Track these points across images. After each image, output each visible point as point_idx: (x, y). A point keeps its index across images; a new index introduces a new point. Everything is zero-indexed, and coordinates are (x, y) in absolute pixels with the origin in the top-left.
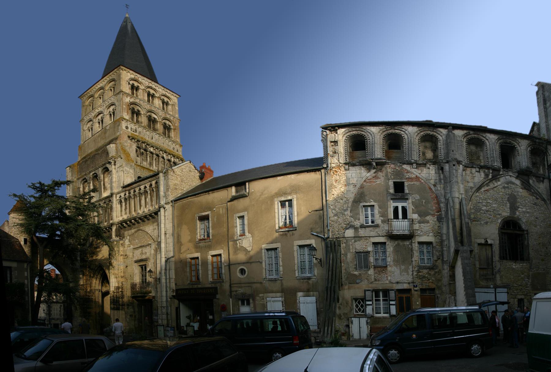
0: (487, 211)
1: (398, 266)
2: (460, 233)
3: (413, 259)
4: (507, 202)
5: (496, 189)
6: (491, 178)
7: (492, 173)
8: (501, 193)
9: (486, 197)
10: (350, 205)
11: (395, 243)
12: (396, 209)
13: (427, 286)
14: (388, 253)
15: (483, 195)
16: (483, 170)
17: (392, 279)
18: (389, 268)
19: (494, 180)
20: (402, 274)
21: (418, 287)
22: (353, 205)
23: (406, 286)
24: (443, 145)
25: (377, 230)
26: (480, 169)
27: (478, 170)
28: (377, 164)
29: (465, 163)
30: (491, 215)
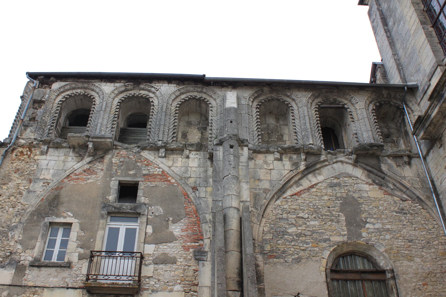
0: (299, 235)
2: (238, 281)
4: (340, 214)
5: (314, 190)
6: (304, 170)
7: (305, 160)
8: (326, 198)
9: (295, 207)
15: (289, 204)
16: (289, 155)
19: (309, 173)
22: (30, 221)
24: (217, 115)
25: (65, 273)
26: (281, 154)
27: (277, 155)
28: (96, 148)
29: (254, 145)
30: (307, 243)
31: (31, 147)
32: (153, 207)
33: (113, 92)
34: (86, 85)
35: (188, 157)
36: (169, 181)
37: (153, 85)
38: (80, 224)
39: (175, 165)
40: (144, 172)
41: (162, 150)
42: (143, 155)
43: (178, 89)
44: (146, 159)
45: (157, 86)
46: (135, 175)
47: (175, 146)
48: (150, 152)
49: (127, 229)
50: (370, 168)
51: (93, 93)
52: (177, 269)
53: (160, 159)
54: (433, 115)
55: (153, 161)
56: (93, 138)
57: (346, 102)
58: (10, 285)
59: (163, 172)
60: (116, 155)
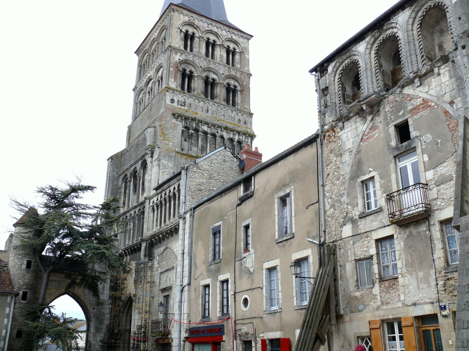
3: (435, 256)
11: (406, 233)
14: (397, 253)
17: (406, 298)
18: (401, 280)
20: (420, 288)
21: (448, 310)
23: (427, 310)
31: (333, 129)
32: (423, 137)
33: (366, 48)
34: (348, 54)
37: (392, 21)
38: (379, 174)
39: (431, 88)
40: (410, 108)
41: (417, 80)
42: (405, 93)
43: (412, 11)
44: (408, 95)
45: (395, 20)
46: (404, 115)
47: (425, 71)
48: (409, 86)
49: (412, 164)
53: (418, 89)
55: (414, 94)
56: (363, 101)
60: (386, 103)
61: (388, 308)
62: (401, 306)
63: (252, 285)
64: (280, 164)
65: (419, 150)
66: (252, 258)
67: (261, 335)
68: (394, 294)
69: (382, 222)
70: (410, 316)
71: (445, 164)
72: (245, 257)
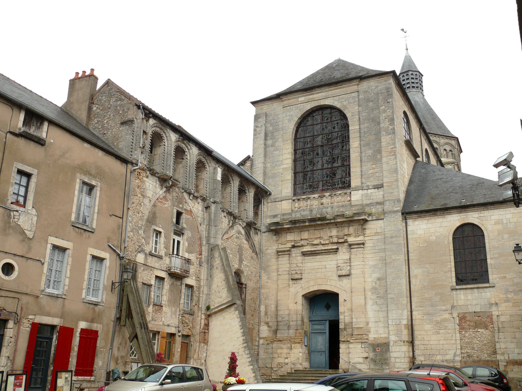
1: (171, 307)
10: (144, 223)
12: (174, 240)
13: (187, 333)
17: (165, 321)
18: (164, 308)
23: (173, 330)
34: (163, 128)
35: (198, 203)
36: (192, 216)
37: (190, 144)
41: (192, 196)
50: (247, 231)
51: (164, 135)
52: (194, 268)
54: (285, 226)
56: (173, 179)
57: (247, 189)
58: (144, 264)
59: (190, 209)
61: (155, 323)
62: (162, 324)
63: (27, 253)
64: (86, 145)
65: (185, 237)
66: (32, 220)
67: (30, 317)
68: (159, 316)
69: (161, 267)
70: (165, 332)
71: (193, 255)
72: (17, 211)
